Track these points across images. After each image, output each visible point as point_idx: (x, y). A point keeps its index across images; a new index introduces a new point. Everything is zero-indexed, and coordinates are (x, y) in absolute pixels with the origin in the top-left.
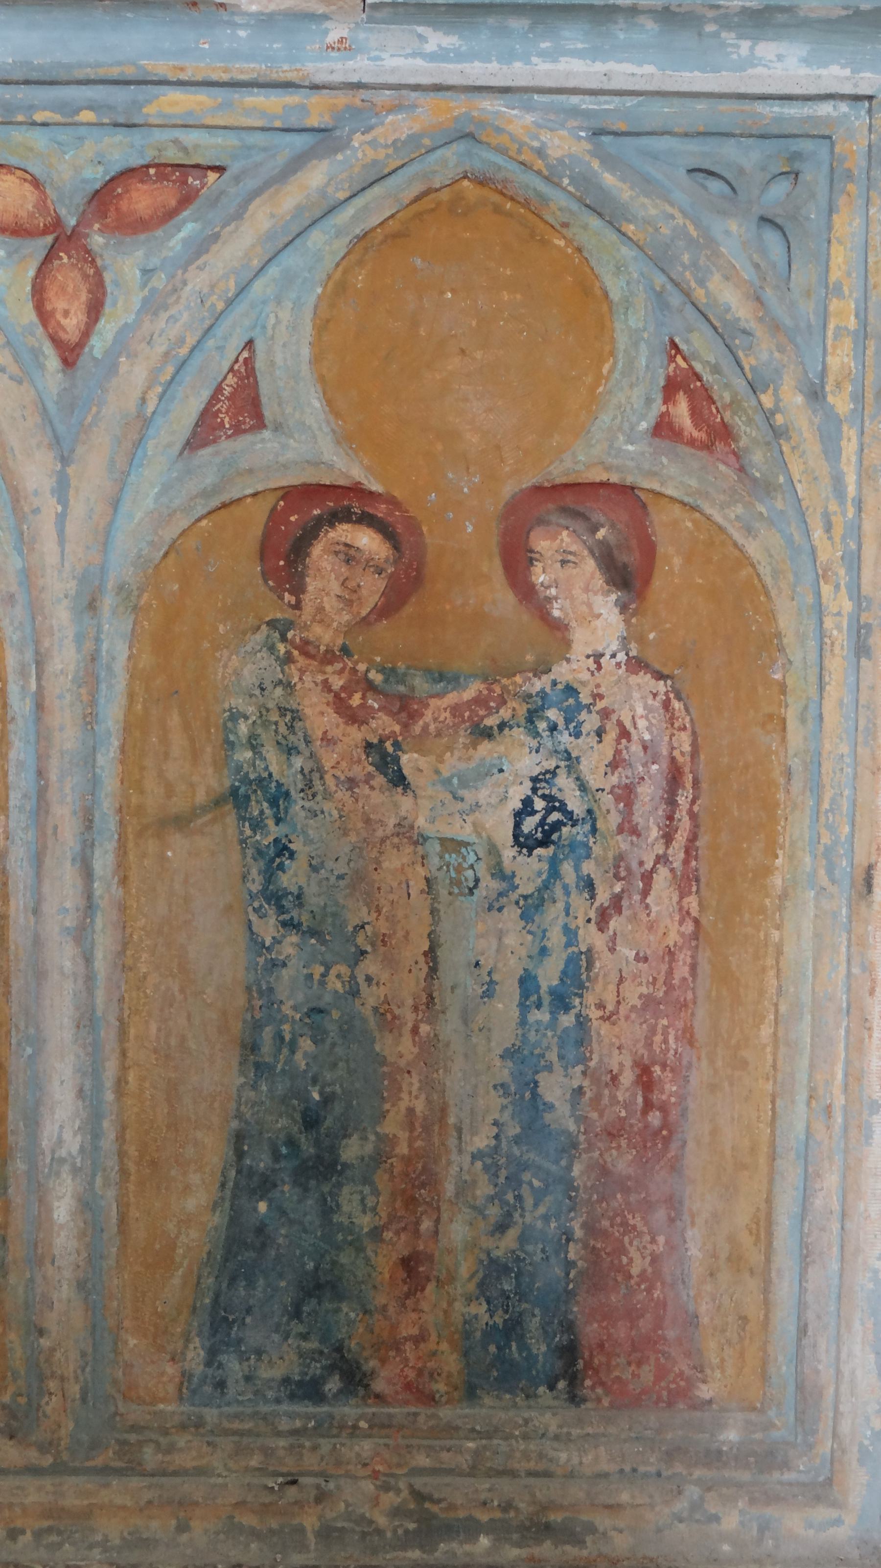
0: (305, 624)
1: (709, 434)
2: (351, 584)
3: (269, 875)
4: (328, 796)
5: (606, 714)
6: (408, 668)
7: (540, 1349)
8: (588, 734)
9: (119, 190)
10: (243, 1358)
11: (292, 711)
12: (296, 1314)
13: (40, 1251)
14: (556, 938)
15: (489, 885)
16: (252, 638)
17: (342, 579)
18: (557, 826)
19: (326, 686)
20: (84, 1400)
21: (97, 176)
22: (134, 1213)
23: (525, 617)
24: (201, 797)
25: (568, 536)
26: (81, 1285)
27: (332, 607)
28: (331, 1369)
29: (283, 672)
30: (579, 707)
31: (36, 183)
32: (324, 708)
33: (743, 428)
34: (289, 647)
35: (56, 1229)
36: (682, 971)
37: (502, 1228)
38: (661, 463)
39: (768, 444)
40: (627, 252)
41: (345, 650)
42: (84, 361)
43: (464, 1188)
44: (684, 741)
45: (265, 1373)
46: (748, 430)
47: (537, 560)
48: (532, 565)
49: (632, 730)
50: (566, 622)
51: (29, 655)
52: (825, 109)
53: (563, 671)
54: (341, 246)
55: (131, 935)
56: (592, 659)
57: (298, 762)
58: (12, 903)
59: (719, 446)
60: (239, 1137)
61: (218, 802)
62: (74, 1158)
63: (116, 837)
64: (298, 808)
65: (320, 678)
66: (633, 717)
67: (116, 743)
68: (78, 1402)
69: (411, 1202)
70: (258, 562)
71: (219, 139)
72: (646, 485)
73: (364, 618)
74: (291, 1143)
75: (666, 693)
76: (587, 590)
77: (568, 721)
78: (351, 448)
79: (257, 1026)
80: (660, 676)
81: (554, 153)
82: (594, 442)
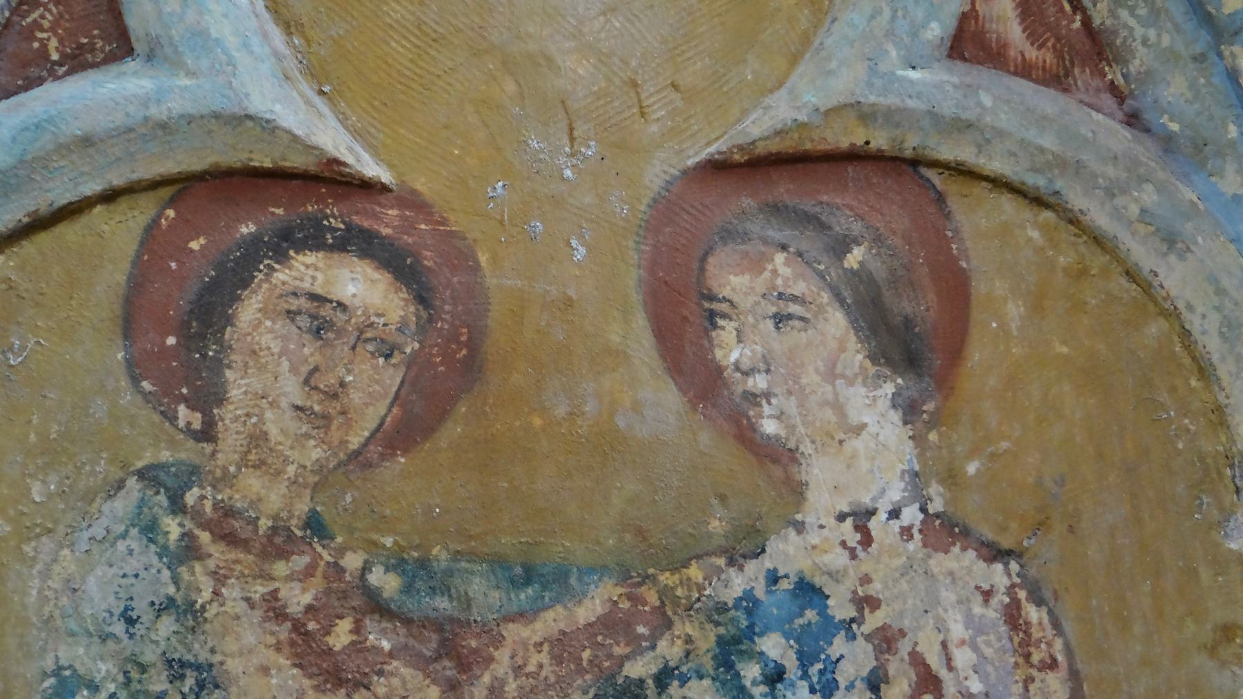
0: (225, 469)
1: (1059, 56)
2: (327, 381)
5: (885, 640)
6: (457, 555)
8: (850, 687)
11: (198, 668)
16: (106, 508)
17: (305, 369)
19: (274, 609)
23: (705, 438)
25: (787, 263)
27: (283, 432)
29: (176, 580)
30: (829, 627)
32: (271, 656)
33: (1139, 31)
34: (189, 525)
38: (979, 104)
39: (1200, 59)
41: (315, 526)
46: (1152, 33)
47: (724, 316)
48: (715, 326)
49: (943, 673)
50: (791, 445)
53: (791, 550)
56: (849, 522)
59: (1081, 76)
65: (259, 590)
66: (944, 645)
70: (120, 342)
72: (946, 152)
73: (357, 453)
75: (1011, 590)
76: (831, 375)
77: (805, 660)
78: (321, 93)
80: (995, 553)
82: (833, 65)
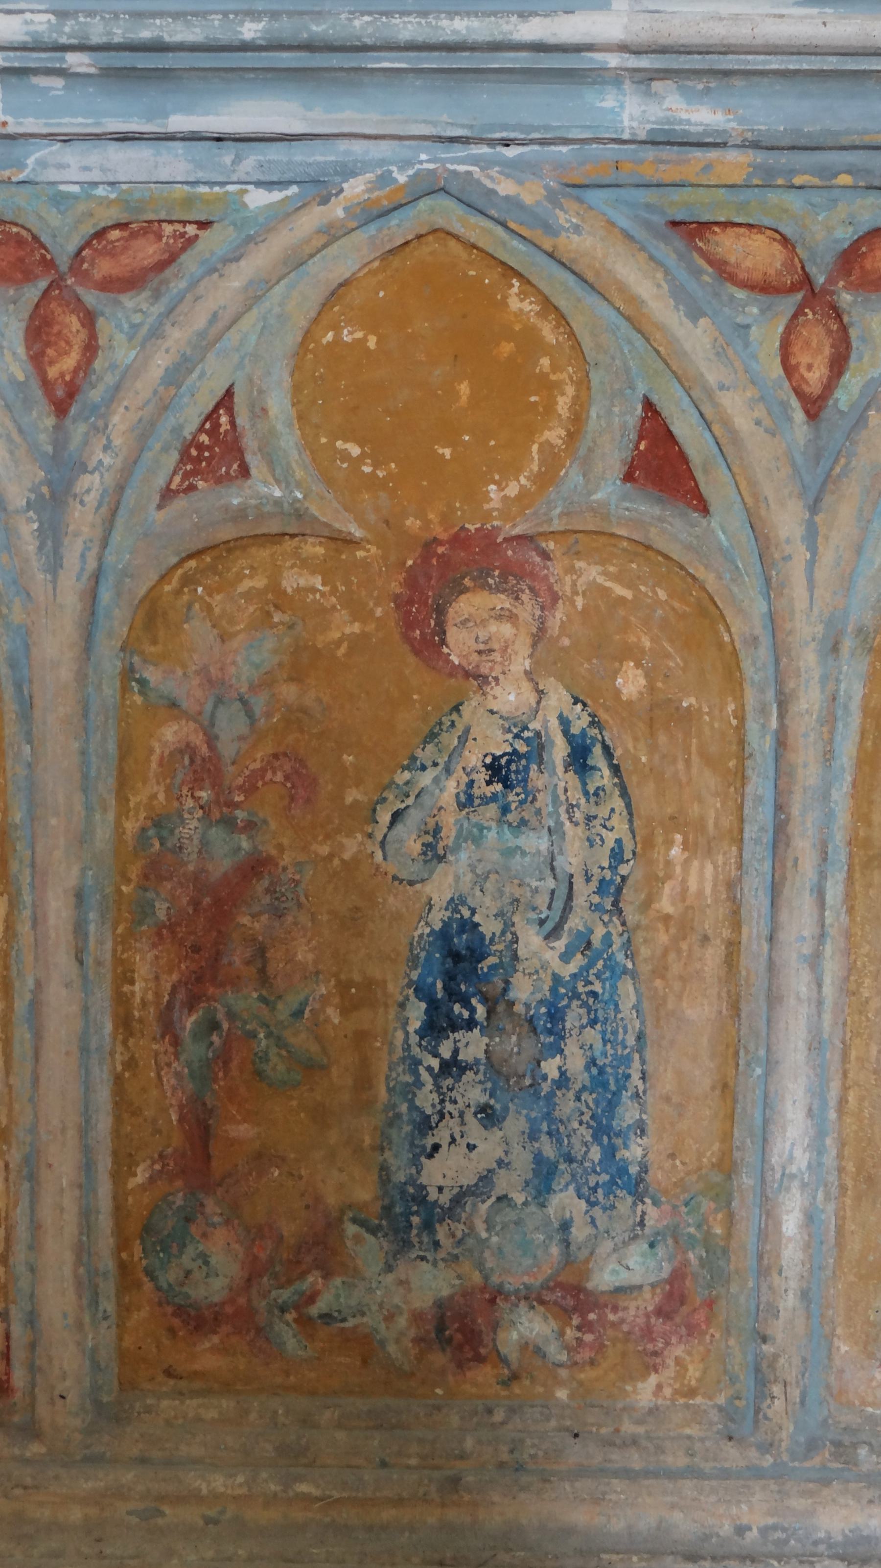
9: (864, 249)
13: (766, 1262)
20: (803, 1403)
21: (845, 235)
22: (850, 1226)
26: (805, 1295)
31: (785, 241)
35: (784, 1241)
42: (826, 414)
51: (770, 694)
55: (855, 962)
58: (745, 930)
62: (803, 1174)
63: (846, 868)
67: (849, 779)
68: (798, 1406)
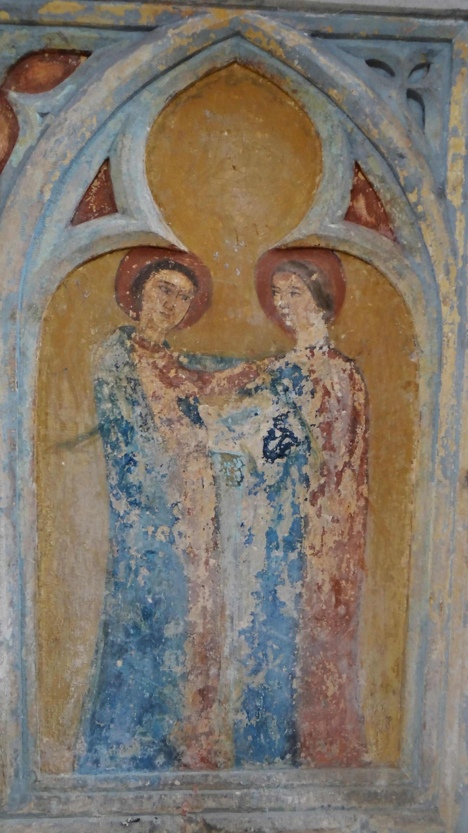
0: (142, 329)
1: (376, 220)
2: (169, 306)
3: (122, 475)
4: (156, 429)
6: (203, 354)
7: (276, 737)
8: (306, 393)
9: (27, 66)
10: (109, 746)
11: (135, 380)
12: (140, 722)
14: (287, 510)
15: (250, 480)
16: (111, 337)
17: (164, 302)
18: (288, 446)
19: (155, 366)
20: (17, 775)
22: (45, 668)
23: (271, 326)
24: (82, 430)
25: (295, 278)
27: (158, 319)
28: (160, 751)
29: (129, 357)
30: (301, 378)
32: (154, 378)
33: (397, 215)
34: (133, 342)
36: (358, 527)
37: (255, 672)
38: (351, 235)
39: (412, 224)
40: (331, 108)
41: (166, 345)
43: (234, 650)
44: (361, 397)
45: (121, 755)
46: (400, 216)
47: (277, 292)
48: (274, 295)
49: (331, 391)
50: (294, 328)
52: (449, 22)
53: (292, 357)
54: (161, 102)
55: (41, 510)
56: (309, 350)
57: (138, 410)
59: (382, 226)
60: (106, 625)
61: (92, 433)
62: (8, 641)
63: (31, 454)
64: (138, 436)
65: (151, 361)
66: (332, 383)
67: (30, 399)
68: (13, 778)
69: (204, 659)
70: (114, 292)
71: (87, 33)
72: (341, 248)
73: (177, 326)
74: (136, 627)
75: (351, 370)
76: (306, 309)
77: (294, 386)
78: (168, 225)
79: (116, 561)
80: (348, 360)
81: (290, 44)
82: (311, 222)
